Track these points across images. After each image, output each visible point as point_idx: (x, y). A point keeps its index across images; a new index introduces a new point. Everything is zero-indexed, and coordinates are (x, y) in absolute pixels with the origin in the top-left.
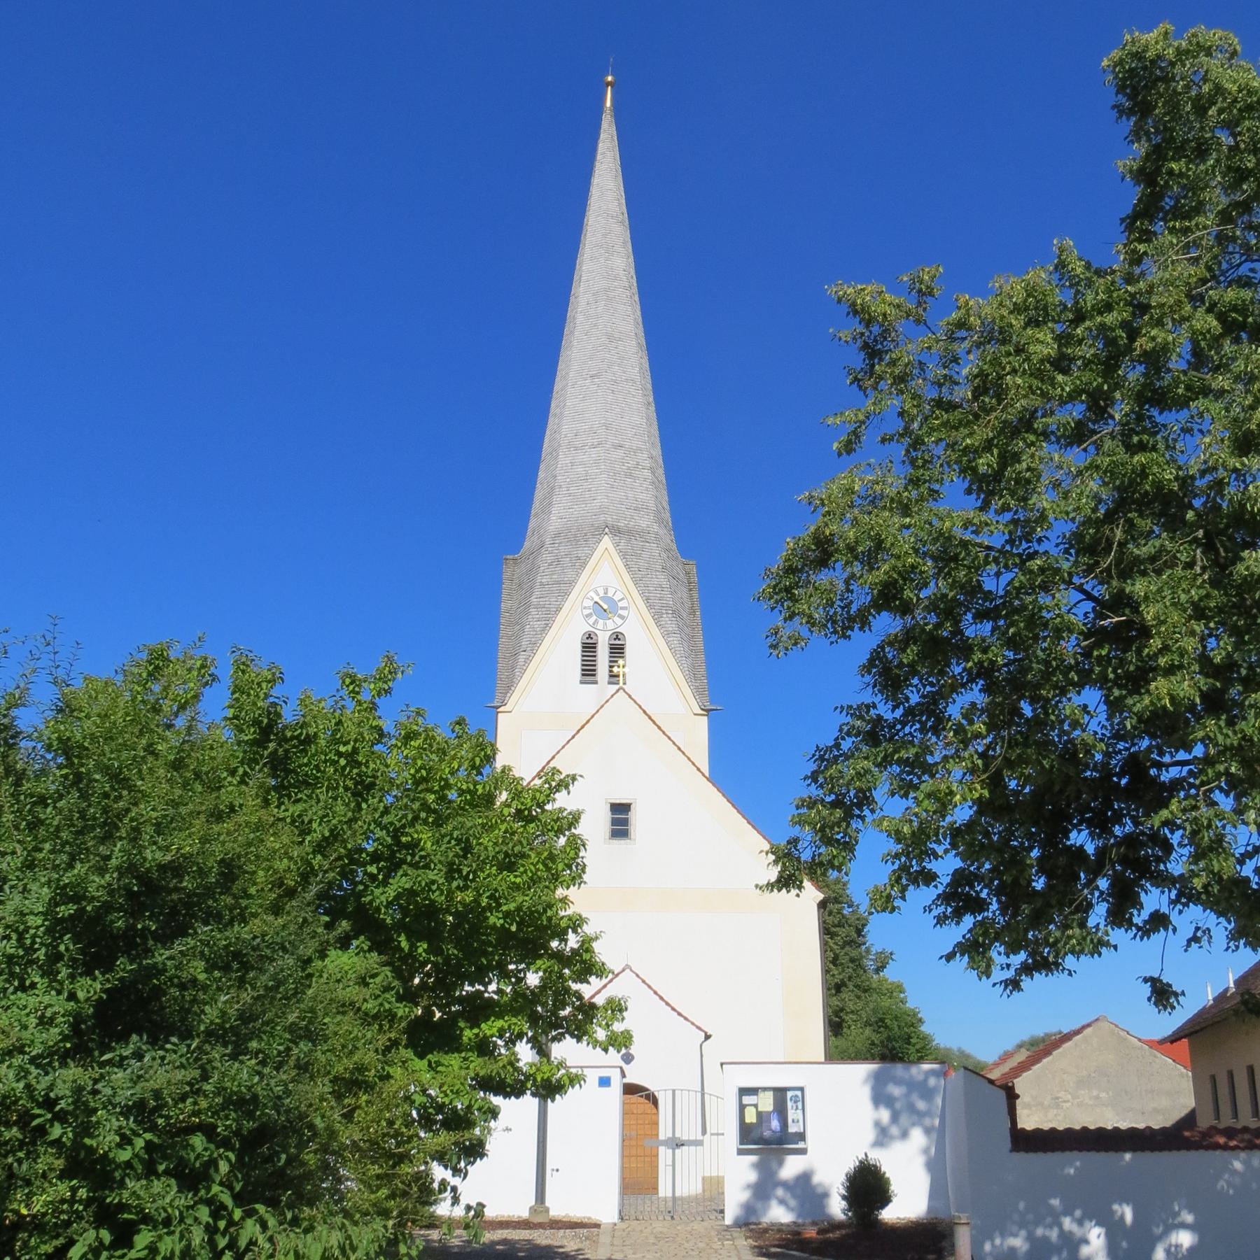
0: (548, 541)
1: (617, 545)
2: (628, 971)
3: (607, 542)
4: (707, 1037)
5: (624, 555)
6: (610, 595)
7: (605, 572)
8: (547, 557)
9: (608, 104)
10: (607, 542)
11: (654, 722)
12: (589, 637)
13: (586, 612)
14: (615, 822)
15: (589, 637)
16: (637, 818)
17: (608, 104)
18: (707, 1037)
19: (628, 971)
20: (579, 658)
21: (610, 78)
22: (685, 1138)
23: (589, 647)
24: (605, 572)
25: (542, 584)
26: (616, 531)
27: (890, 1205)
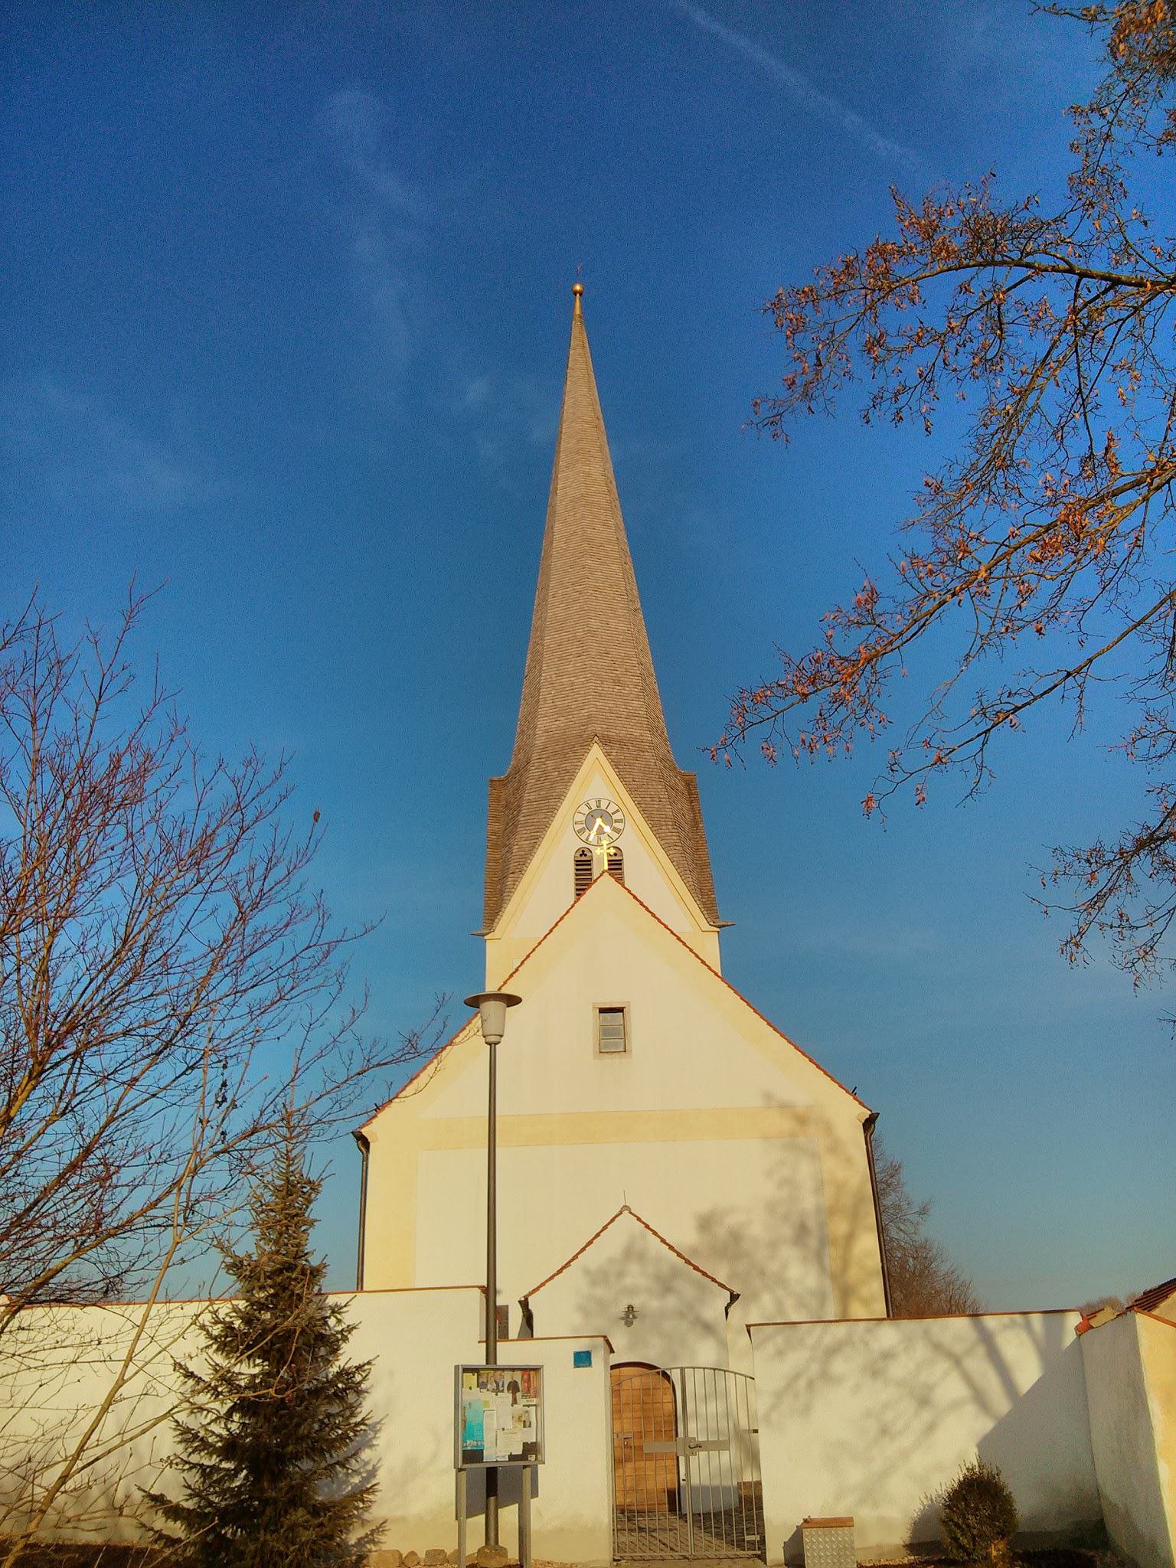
0: (535, 756)
1: (607, 754)
2: (626, 1212)
3: (596, 752)
4: (734, 1297)
5: (616, 765)
6: (603, 807)
7: (596, 780)
8: (534, 771)
9: (578, 312)
10: (596, 752)
11: (647, 909)
12: (583, 854)
13: (578, 827)
14: (606, 1032)
15: (583, 854)
16: (637, 1022)
17: (578, 312)
18: (734, 1297)
19: (626, 1212)
20: (572, 877)
21: (578, 288)
22: (702, 1438)
23: (583, 864)
24: (596, 780)
25: (530, 801)
26: (606, 741)
27: (1003, 1479)
